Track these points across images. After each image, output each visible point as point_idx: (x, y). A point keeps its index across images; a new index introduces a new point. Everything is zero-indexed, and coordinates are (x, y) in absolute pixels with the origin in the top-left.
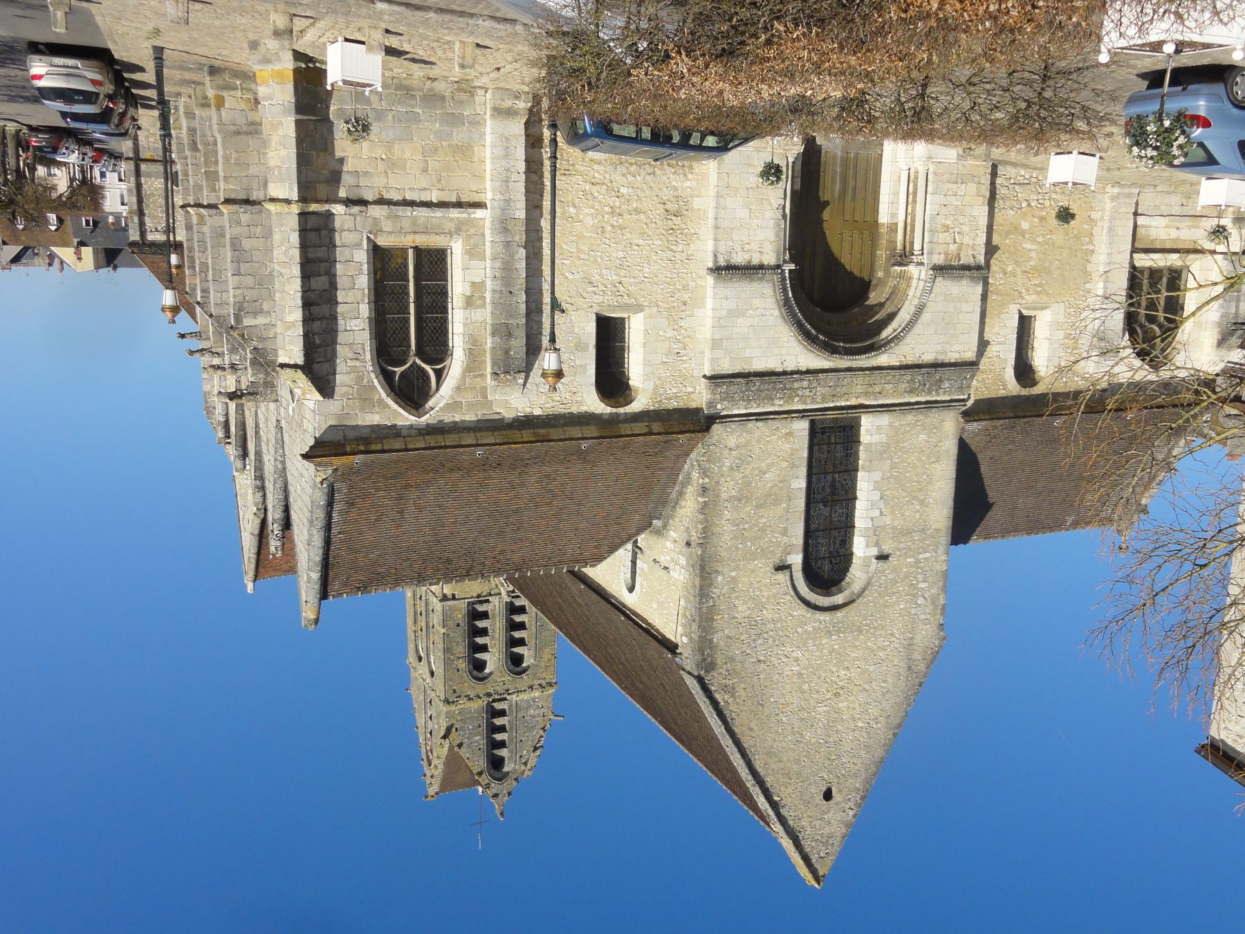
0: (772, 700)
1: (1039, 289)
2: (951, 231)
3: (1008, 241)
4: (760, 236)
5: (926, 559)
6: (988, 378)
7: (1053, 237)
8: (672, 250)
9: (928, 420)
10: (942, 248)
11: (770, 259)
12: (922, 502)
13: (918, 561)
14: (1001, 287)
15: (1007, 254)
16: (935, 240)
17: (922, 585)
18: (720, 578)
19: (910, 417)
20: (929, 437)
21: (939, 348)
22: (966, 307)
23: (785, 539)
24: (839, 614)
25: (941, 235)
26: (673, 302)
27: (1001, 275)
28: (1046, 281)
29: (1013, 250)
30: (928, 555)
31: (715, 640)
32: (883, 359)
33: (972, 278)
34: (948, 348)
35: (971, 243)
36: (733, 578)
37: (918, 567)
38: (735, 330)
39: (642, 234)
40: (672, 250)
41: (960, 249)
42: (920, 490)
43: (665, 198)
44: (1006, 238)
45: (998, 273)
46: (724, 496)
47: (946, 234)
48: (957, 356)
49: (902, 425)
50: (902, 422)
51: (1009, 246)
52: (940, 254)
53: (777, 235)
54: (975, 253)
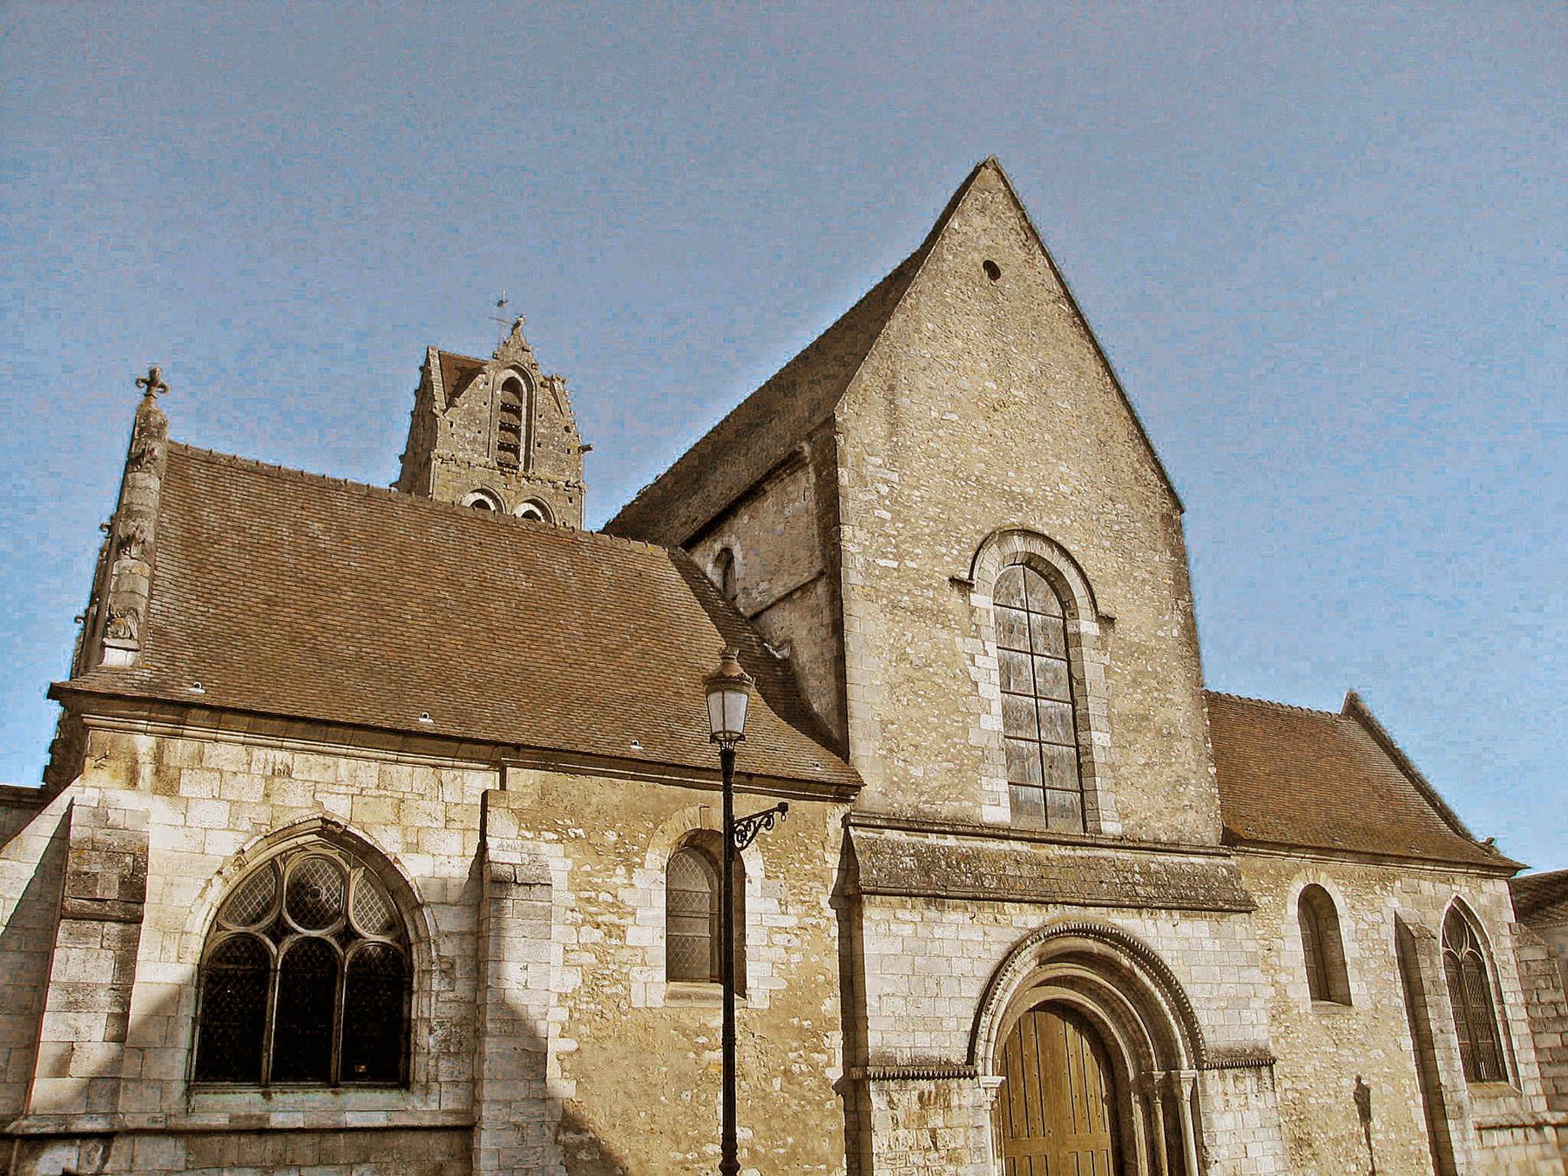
0: (1088, 441)
1: (702, 1040)
2: (943, 1153)
3: (790, 1140)
4: (1229, 1117)
5: (884, 556)
6: (801, 861)
7: (679, 1156)
8: (1297, 1091)
9: (913, 799)
10: (957, 1118)
11: (1214, 1083)
12: (903, 657)
13: (899, 557)
14: (795, 1044)
15: (789, 1112)
16: (971, 1133)
17: (888, 516)
18: (1175, 633)
19: (946, 809)
20: (905, 770)
21: (938, 932)
22: (890, 1005)
23: (1107, 661)
24: (1015, 520)
25: (961, 1142)
26: (1285, 1021)
27: (796, 1068)
28: (685, 1057)
29: (775, 1123)
30: (882, 562)
31: (1169, 553)
32: (1032, 918)
33: (890, 1060)
34: (922, 931)
35: (902, 1132)
36: (1160, 627)
37: (896, 547)
38: (1235, 979)
39: (1329, 1110)
40: (1297, 1091)
41: (922, 1119)
42: (909, 679)
43: (1314, 1163)
44: (793, 1147)
45: (802, 1073)
46: (1188, 744)
47: (952, 1145)
48: (903, 914)
49: (957, 799)
50: (957, 804)
51: (783, 1130)
52: (960, 1107)
53: (1209, 1120)
54: (890, 1112)
